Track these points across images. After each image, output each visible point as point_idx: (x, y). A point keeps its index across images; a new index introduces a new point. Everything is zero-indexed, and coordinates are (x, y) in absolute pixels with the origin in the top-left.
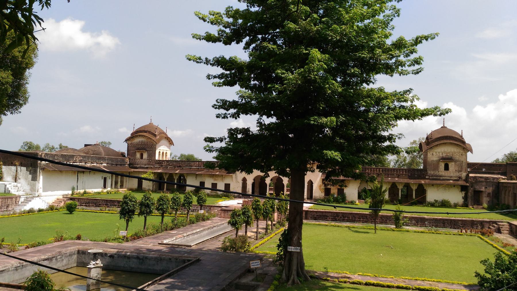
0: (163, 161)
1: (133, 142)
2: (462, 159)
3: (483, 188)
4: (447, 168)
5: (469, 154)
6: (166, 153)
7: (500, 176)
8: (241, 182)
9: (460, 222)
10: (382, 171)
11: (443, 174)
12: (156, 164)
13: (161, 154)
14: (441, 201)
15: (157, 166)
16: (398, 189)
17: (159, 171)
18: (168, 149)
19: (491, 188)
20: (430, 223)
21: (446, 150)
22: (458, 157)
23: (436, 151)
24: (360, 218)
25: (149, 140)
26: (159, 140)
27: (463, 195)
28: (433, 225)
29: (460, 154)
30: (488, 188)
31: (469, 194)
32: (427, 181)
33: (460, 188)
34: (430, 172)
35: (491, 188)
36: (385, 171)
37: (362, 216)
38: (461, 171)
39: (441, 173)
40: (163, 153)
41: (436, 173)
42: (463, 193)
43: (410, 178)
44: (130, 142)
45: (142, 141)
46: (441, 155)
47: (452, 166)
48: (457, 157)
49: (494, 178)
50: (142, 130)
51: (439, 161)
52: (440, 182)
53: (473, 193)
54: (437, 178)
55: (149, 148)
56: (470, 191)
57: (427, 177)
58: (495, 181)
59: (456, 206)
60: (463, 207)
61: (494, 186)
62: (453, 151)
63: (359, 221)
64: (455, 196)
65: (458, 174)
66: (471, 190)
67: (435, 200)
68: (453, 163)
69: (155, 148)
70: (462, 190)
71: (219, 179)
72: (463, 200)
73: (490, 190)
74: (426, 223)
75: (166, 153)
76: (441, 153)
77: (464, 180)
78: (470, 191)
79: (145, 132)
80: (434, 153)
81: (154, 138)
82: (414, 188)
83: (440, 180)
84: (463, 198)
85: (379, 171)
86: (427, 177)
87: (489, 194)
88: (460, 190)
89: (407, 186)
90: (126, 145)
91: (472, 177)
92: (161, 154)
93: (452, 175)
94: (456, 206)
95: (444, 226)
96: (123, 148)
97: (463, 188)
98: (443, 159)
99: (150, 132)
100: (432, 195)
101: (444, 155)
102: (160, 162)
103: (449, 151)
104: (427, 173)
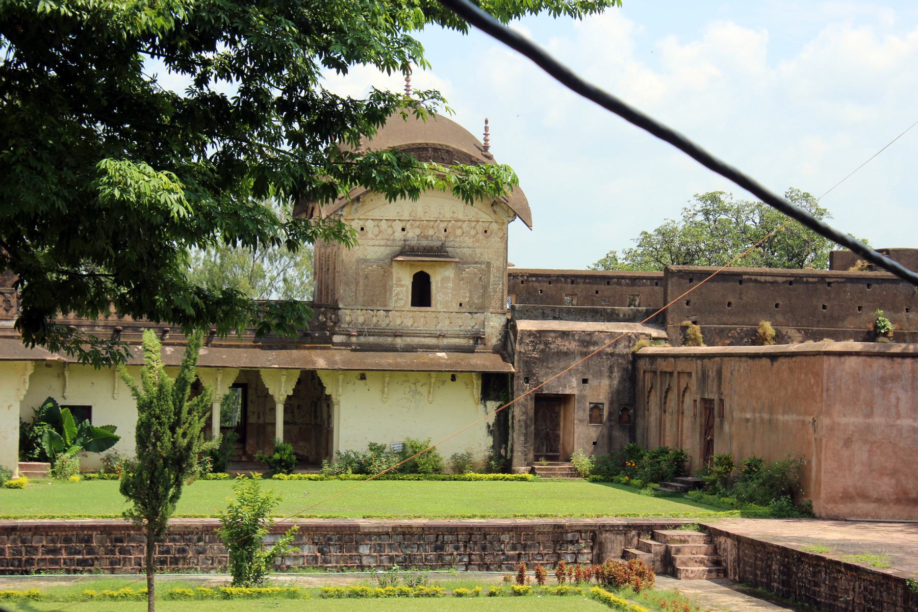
2: (486, 252)
3: (574, 382)
4: (422, 293)
5: (516, 227)
7: (638, 328)
9: (505, 537)
11: (409, 322)
14: (399, 448)
19: (605, 382)
20: (380, 548)
21: (420, 213)
22: (469, 241)
23: (376, 214)
24: (55, 551)
27: (492, 419)
28: (391, 559)
30: (593, 382)
32: (340, 357)
33: (477, 384)
34: (352, 316)
35: (605, 382)
37: (67, 540)
38: (482, 309)
41: (380, 319)
42: (493, 406)
46: (399, 235)
47: (442, 282)
48: (464, 243)
49: (616, 339)
51: (392, 258)
52: (389, 360)
53: (531, 405)
57: (337, 339)
58: (621, 349)
59: (460, 468)
60: (489, 470)
61: (616, 374)
62: (448, 215)
63: (53, 565)
64: (459, 424)
65: (469, 323)
67: (373, 447)
70: (486, 396)
72: (490, 441)
73: (601, 390)
74: (364, 550)
76: (398, 226)
77: (496, 350)
80: (369, 225)
82: (281, 390)
83: (392, 349)
87: (596, 407)
88: (477, 392)
89: (248, 385)
91: (530, 333)
93: (443, 326)
95: (440, 558)
97: (494, 386)
100: (361, 421)
101: (412, 234)
103: (433, 214)
104: (337, 322)
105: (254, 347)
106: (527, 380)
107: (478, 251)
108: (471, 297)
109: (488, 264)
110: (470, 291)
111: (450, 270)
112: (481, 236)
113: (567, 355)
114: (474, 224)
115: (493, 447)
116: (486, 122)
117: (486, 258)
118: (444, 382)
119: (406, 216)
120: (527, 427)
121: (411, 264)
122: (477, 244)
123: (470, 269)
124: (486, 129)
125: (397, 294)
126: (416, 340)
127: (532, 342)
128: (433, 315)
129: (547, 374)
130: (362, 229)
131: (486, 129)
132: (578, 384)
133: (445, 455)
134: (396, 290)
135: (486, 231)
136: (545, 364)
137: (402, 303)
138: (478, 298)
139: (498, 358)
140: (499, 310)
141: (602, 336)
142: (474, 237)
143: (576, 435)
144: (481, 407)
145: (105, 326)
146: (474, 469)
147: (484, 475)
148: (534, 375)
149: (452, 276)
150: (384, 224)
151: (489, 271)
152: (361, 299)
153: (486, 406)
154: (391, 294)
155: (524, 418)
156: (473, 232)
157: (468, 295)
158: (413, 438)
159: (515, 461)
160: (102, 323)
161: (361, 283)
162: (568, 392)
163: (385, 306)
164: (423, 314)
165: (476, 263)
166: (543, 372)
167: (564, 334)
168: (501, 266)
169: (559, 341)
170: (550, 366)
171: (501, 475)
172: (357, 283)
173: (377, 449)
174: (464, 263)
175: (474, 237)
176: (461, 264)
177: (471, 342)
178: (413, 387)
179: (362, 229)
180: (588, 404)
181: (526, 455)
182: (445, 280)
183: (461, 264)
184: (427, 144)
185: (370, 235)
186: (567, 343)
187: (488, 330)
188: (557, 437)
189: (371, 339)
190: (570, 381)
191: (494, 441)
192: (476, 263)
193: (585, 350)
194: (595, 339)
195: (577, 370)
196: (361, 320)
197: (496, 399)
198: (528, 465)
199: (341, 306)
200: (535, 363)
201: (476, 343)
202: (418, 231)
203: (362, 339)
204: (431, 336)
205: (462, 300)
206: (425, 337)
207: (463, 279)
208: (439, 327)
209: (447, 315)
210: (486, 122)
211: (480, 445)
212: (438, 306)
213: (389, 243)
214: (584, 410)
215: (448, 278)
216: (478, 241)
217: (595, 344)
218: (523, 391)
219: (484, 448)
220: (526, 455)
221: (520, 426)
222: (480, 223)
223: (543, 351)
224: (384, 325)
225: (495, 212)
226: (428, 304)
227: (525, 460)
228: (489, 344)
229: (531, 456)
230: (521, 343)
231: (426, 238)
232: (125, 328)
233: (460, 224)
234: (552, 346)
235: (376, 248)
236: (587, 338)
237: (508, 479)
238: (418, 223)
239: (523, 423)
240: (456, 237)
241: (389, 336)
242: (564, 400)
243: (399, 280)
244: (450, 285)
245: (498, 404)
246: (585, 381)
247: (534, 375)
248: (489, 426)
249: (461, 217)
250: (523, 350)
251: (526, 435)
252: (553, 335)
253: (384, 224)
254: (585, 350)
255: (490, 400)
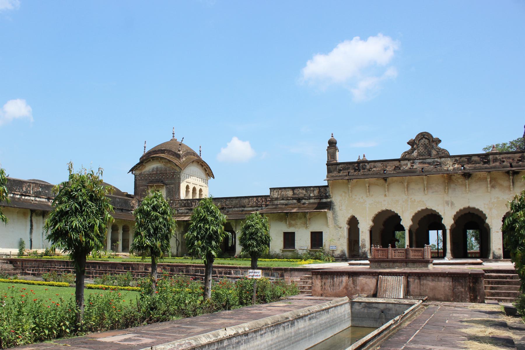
0: (193, 200)
1: (144, 171)
6: (201, 190)
8: (345, 227)
12: (181, 206)
13: (191, 190)
15: (183, 210)
17: (186, 219)
18: (204, 184)
25: (169, 165)
26: (186, 165)
40: (194, 189)
44: (138, 172)
45: (157, 168)
50: (157, 149)
55: (169, 179)
69: (179, 178)
71: (299, 222)
75: (201, 190)
79: (163, 151)
81: (176, 161)
90: (132, 177)
92: (191, 190)
96: (126, 184)
99: (169, 152)
102: (188, 204)
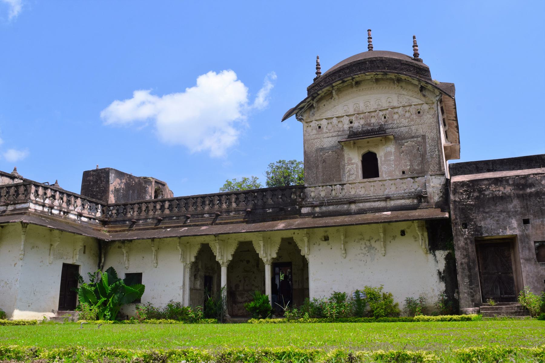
3: (514, 223)
4: (370, 167)
10: (171, 207)
16: (218, 266)
22: (405, 122)
27: (442, 266)
29: (413, 110)
31: (458, 255)
32: (298, 222)
36: (178, 206)
38: (422, 173)
39: (352, 191)
41: (337, 192)
42: (441, 255)
43: (251, 217)
46: (346, 126)
47: (387, 156)
52: (347, 223)
53: (472, 248)
54: (341, 207)
56: (461, 243)
57: (304, 210)
59: (415, 310)
62: (385, 105)
65: (412, 186)
66: (462, 239)
68: (391, 148)
72: (442, 286)
76: (346, 120)
78: (461, 243)
80: (324, 123)
82: (267, 254)
83: (348, 213)
84: (442, 277)
85: (162, 208)
86: (304, 210)
93: (391, 190)
94: (415, 310)
97: (438, 234)
98: (354, 137)
100: (329, 275)
101: (358, 124)
105: (243, 222)
106: (465, 226)
107: (413, 128)
108: (411, 165)
109: (424, 137)
110: (410, 160)
111: (391, 146)
112: (415, 117)
113: (504, 198)
114: (408, 108)
115: (446, 292)
116: (414, 37)
117: (421, 132)
118: (394, 238)
119: (351, 112)
120: (470, 269)
121: (359, 148)
122: (412, 123)
123: (408, 143)
124: (415, 42)
125: (349, 171)
126: (368, 205)
127: (465, 191)
128: (381, 183)
129: (484, 219)
130: (320, 127)
131: (415, 42)
132: (519, 225)
133: (400, 301)
134: (348, 168)
135: (419, 112)
136: (481, 210)
137: (353, 177)
138: (419, 165)
139: (438, 211)
140: (438, 173)
141: (538, 177)
142: (408, 118)
143: (524, 274)
144: (431, 256)
145: (153, 218)
146: (425, 311)
147: (432, 317)
148: (472, 220)
149: (393, 150)
150: (335, 121)
151: (425, 142)
152: (320, 178)
153: (435, 255)
154: (344, 171)
155: (466, 260)
156: (407, 115)
157: (408, 164)
158: (369, 285)
159: (462, 302)
160: (151, 217)
161: (320, 166)
162: (509, 233)
163: (340, 181)
164: (372, 184)
165: (413, 137)
166: (480, 217)
167: (497, 181)
168: (435, 136)
169: (493, 188)
170: (487, 210)
171: (449, 317)
172: (317, 167)
173: (339, 298)
174: (402, 139)
175: (408, 118)
176: (398, 139)
177: (416, 201)
178: (368, 244)
179: (320, 127)
180: (532, 243)
181: (473, 296)
182: (387, 154)
183: (398, 139)
184: (365, 59)
185: (325, 130)
186: (501, 188)
187: (429, 190)
188: (512, 279)
189: (331, 208)
190: (510, 223)
191: (446, 286)
192: (413, 137)
193: (521, 192)
194: (530, 181)
195: (516, 212)
196: (323, 194)
197: (444, 249)
198: (476, 305)
199: (306, 185)
200: (471, 210)
201: (420, 202)
202: (362, 122)
203: (324, 209)
204: (379, 200)
205: (404, 168)
206: (374, 201)
207: (403, 152)
208: (386, 193)
209: (393, 182)
210: (414, 37)
211: (433, 290)
212: (384, 175)
213: (340, 133)
214: (529, 249)
215: (390, 153)
216: (412, 120)
217: (531, 185)
218: (462, 235)
219: (437, 293)
220: (473, 296)
221: (463, 269)
222: (413, 106)
223: (477, 198)
224: (341, 196)
225: (424, 96)
226: (376, 175)
227: (473, 301)
228: (432, 201)
229: (479, 296)
230: (455, 192)
231: (369, 125)
232: (164, 218)
233: (396, 110)
234: (487, 193)
235: (330, 139)
236: (522, 181)
237: (455, 320)
238: (362, 116)
239: (465, 266)
240: (394, 120)
241: (345, 204)
242: (510, 243)
243: (350, 159)
244: (392, 158)
245: (446, 252)
246: (526, 222)
247: (472, 220)
248: (440, 273)
249: (395, 104)
250: (457, 199)
251: (470, 277)
252: (486, 182)
253: (335, 121)
254: (521, 192)
255: (438, 249)
